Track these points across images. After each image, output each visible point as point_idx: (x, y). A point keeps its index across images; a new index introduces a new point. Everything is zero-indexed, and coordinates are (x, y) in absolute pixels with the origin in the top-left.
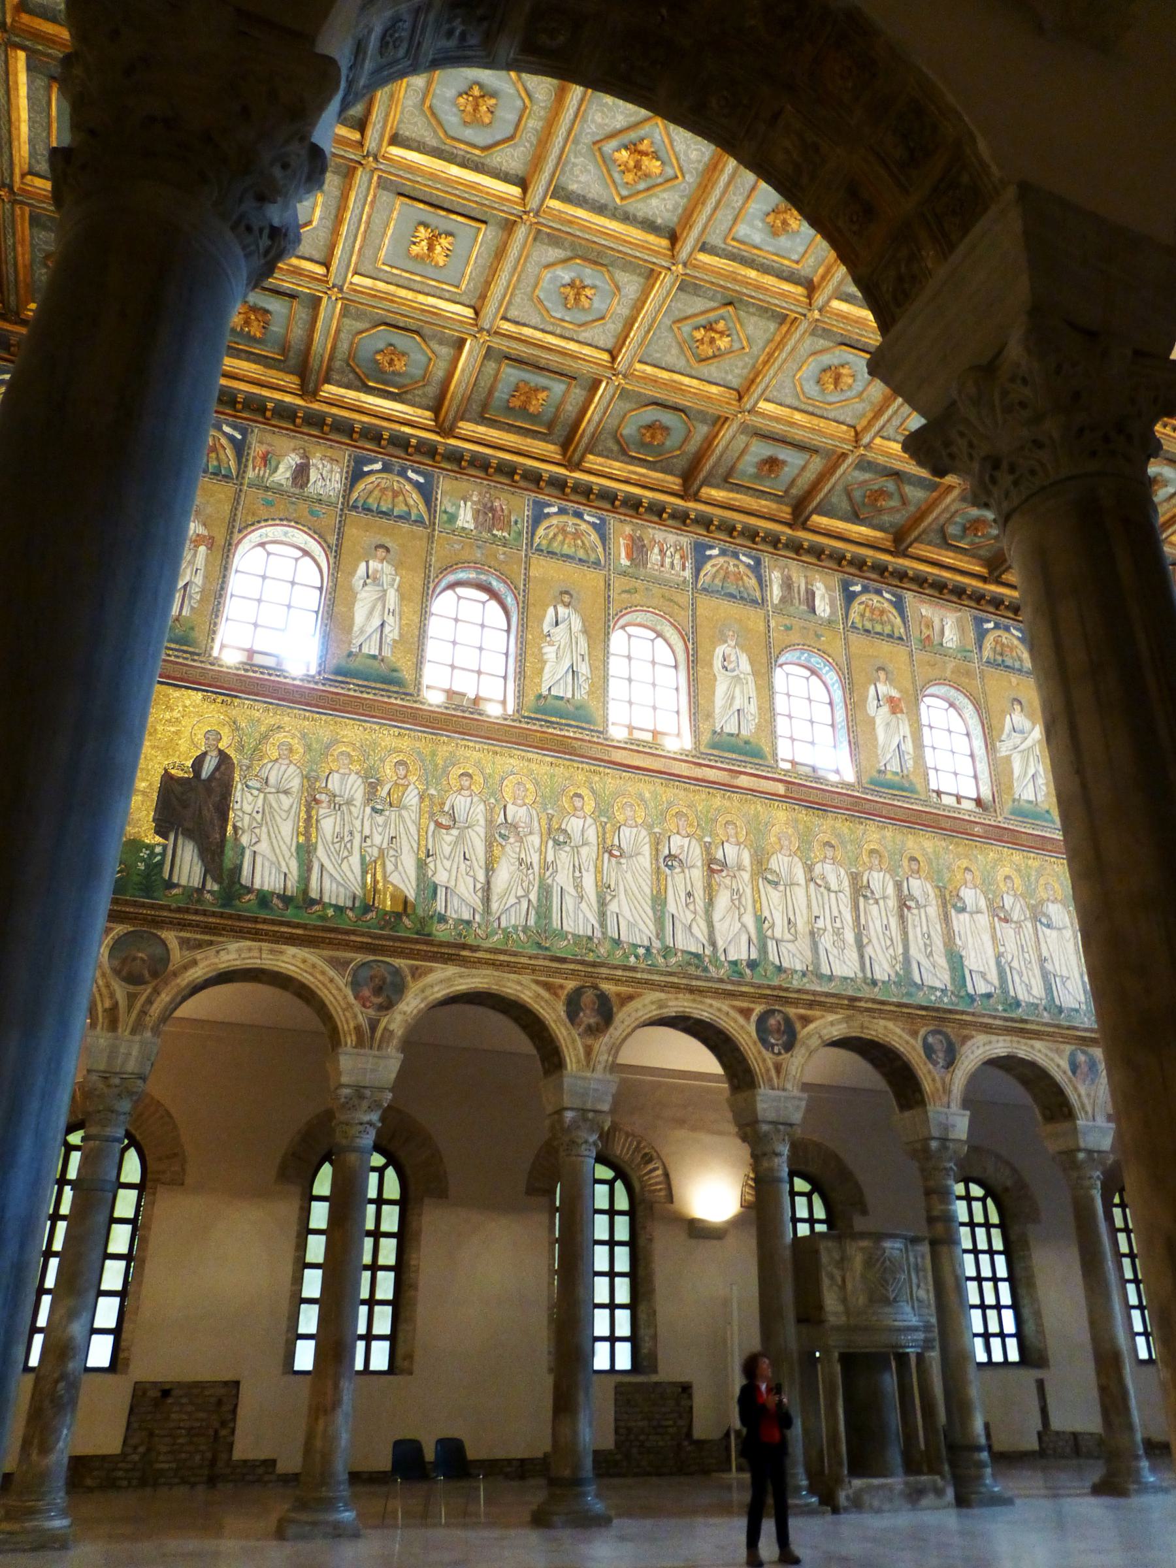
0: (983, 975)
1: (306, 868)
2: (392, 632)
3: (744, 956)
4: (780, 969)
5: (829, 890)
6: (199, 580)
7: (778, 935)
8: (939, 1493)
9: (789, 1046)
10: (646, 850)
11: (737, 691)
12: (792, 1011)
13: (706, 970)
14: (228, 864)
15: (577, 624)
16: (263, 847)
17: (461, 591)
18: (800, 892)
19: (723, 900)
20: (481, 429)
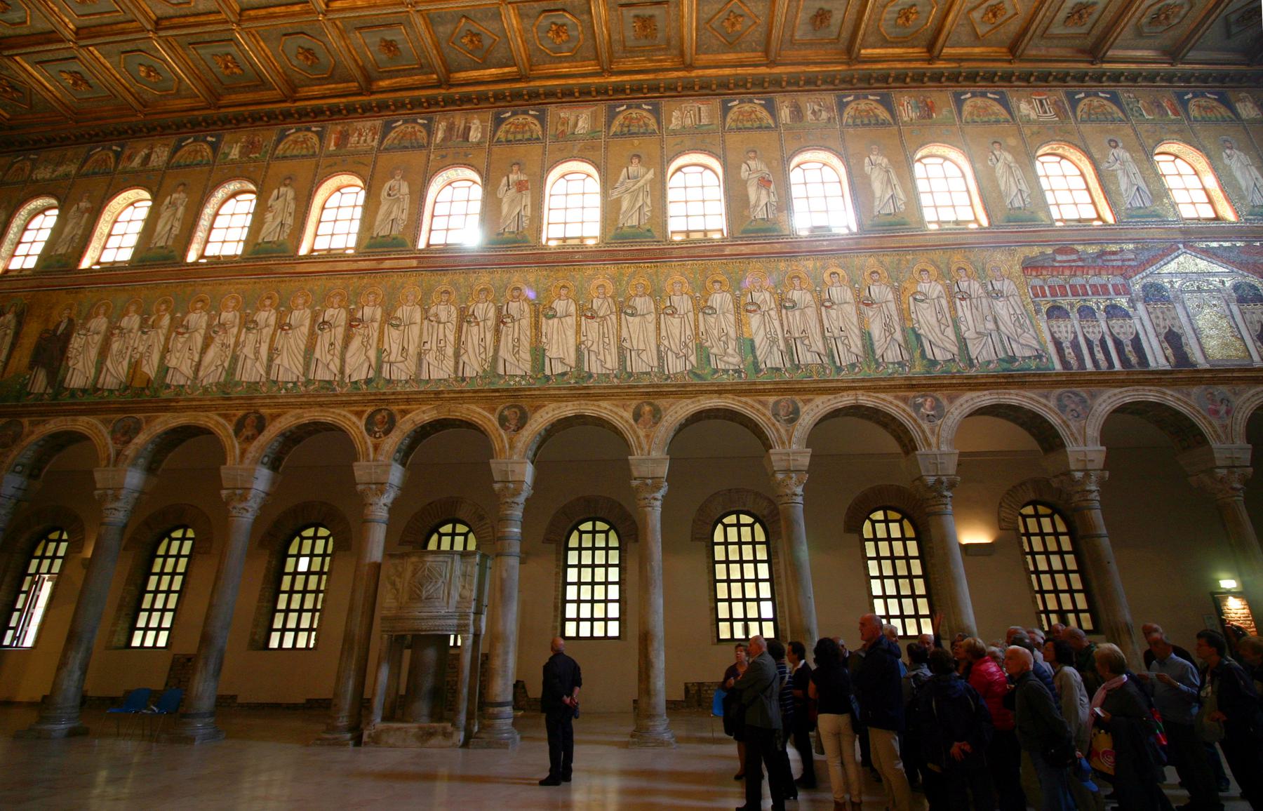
0: (562, 360)
1: (99, 371)
2: (176, 231)
3: (364, 377)
4: (389, 381)
5: (439, 322)
6: (80, 232)
7: (392, 359)
8: (446, 735)
9: (387, 432)
10: (307, 323)
11: (395, 208)
12: (394, 408)
13: (334, 390)
14: (59, 378)
15: (290, 194)
16: (80, 365)
17: (239, 198)
18: (415, 330)
19: (356, 344)
20: (233, 97)
